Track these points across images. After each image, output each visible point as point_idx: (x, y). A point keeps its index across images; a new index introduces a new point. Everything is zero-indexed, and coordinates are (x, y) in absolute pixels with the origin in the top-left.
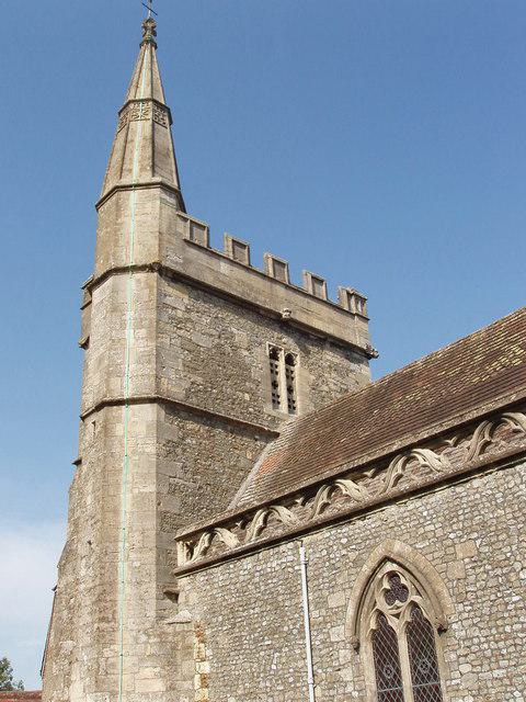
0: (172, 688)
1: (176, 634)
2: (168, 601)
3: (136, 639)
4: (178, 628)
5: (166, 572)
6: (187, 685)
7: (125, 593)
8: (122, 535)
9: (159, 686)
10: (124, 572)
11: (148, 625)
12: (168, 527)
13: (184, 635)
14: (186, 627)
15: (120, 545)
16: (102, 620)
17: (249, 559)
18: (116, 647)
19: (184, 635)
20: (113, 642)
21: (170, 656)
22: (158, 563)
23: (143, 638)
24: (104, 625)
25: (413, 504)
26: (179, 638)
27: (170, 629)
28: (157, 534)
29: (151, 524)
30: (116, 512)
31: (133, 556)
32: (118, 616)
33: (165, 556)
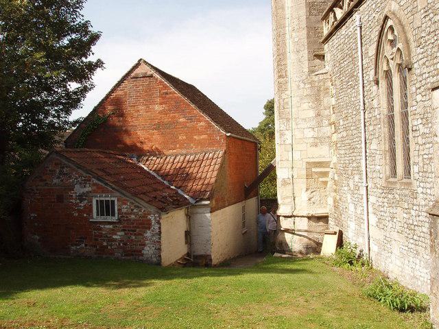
0: (319, 115)
1: (320, 81)
2: (317, 61)
3: (299, 86)
4: (321, 77)
5: (315, 42)
6: (326, 112)
7: (291, 59)
8: (287, 22)
9: (312, 114)
10: (290, 46)
11: (304, 77)
12: (315, 12)
13: (324, 81)
14: (325, 76)
15: (287, 28)
16: (280, 77)
17: (387, 129)
18: (288, 92)
19: (324, 81)
20: (286, 89)
21: (317, 95)
22: (308, 37)
23: (302, 85)
24: (281, 80)
25: (343, 30)
26: (322, 83)
27: (316, 79)
28: (307, 18)
29: (303, 12)
30: (283, 8)
31: (294, 34)
32: (288, 74)
33: (312, 30)
